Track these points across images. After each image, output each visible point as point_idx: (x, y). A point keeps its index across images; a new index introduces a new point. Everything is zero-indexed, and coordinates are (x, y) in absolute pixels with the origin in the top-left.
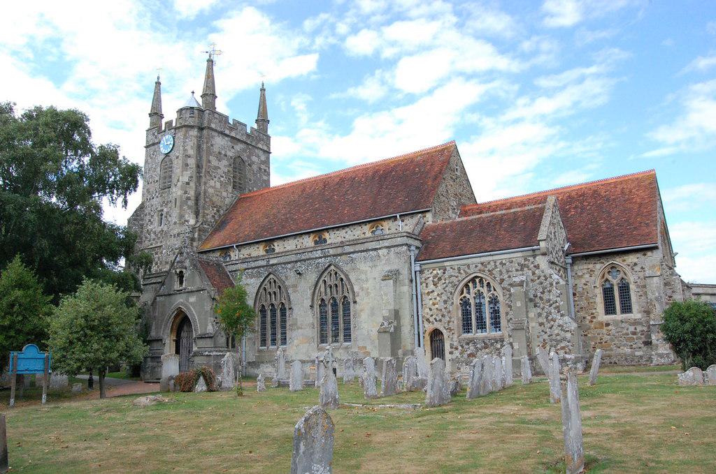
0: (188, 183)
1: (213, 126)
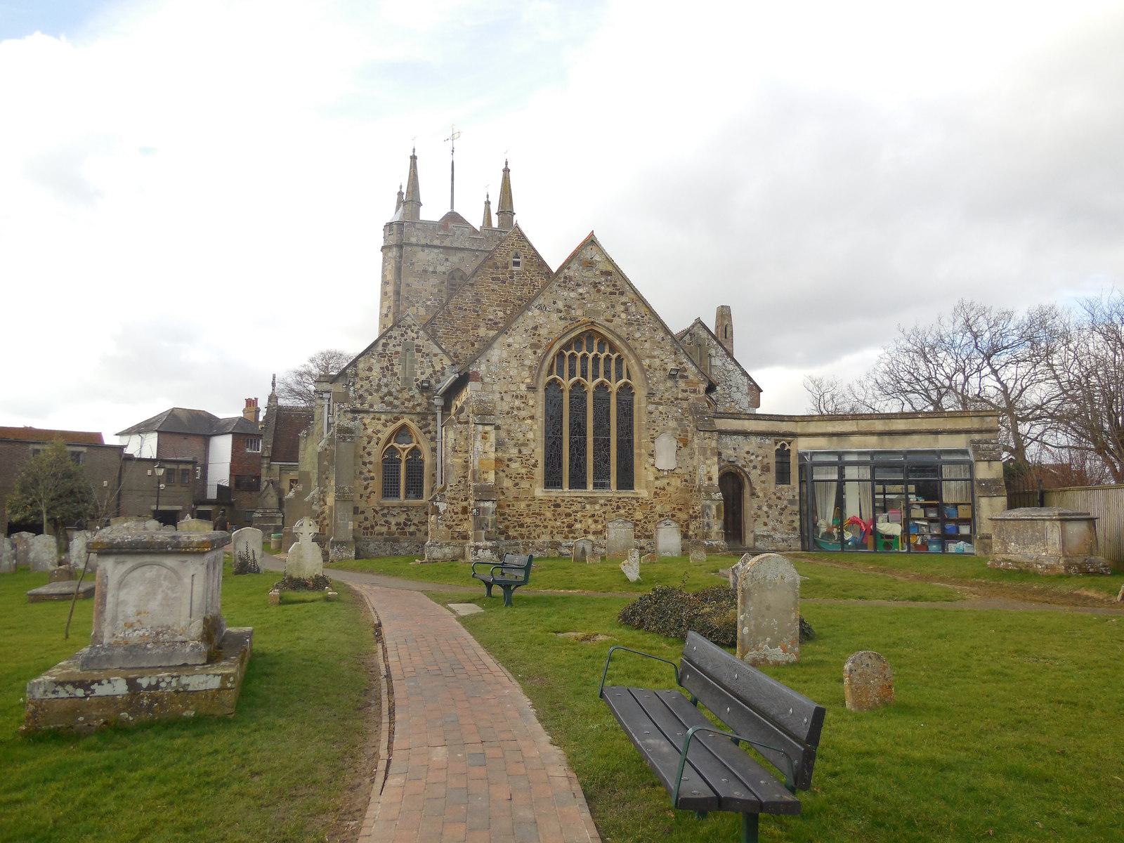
0: (386, 316)
1: (413, 240)
